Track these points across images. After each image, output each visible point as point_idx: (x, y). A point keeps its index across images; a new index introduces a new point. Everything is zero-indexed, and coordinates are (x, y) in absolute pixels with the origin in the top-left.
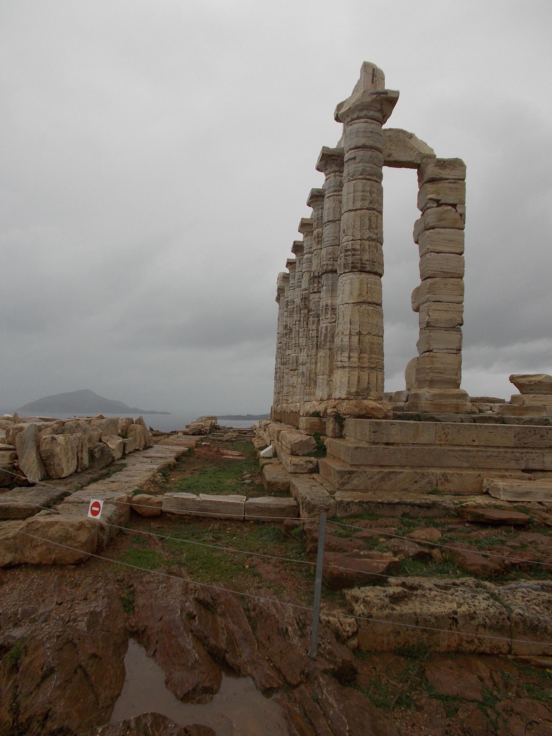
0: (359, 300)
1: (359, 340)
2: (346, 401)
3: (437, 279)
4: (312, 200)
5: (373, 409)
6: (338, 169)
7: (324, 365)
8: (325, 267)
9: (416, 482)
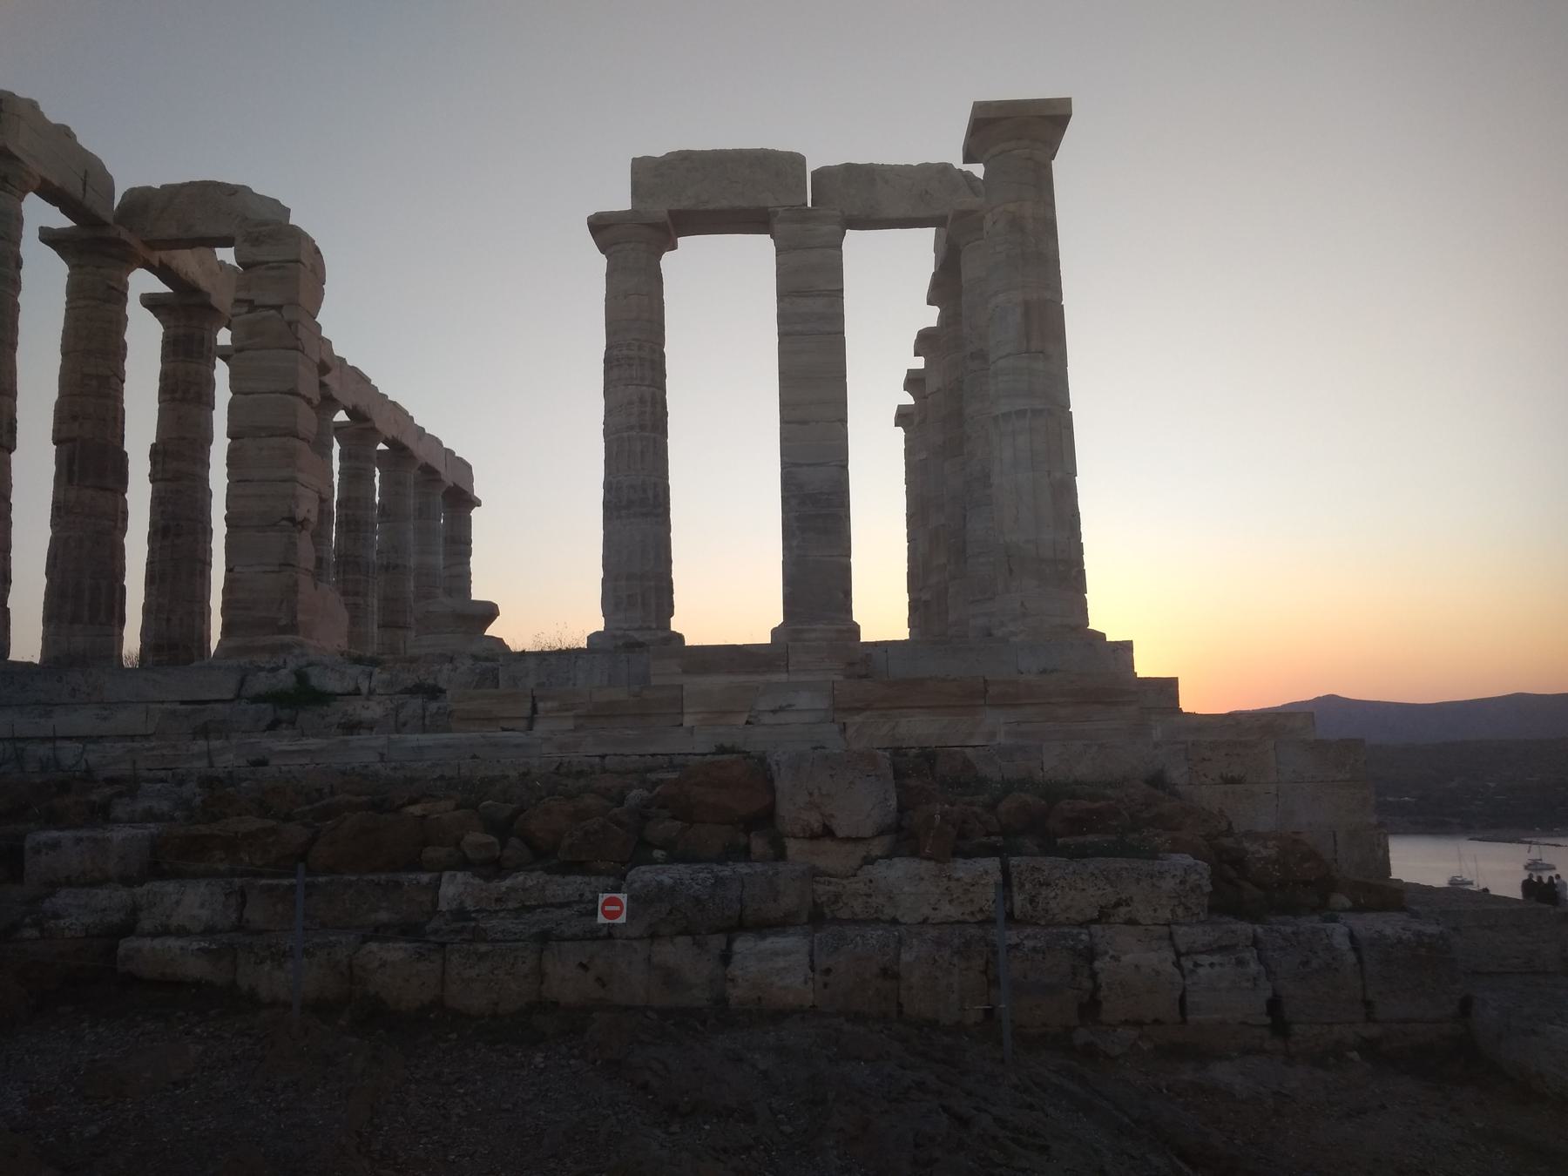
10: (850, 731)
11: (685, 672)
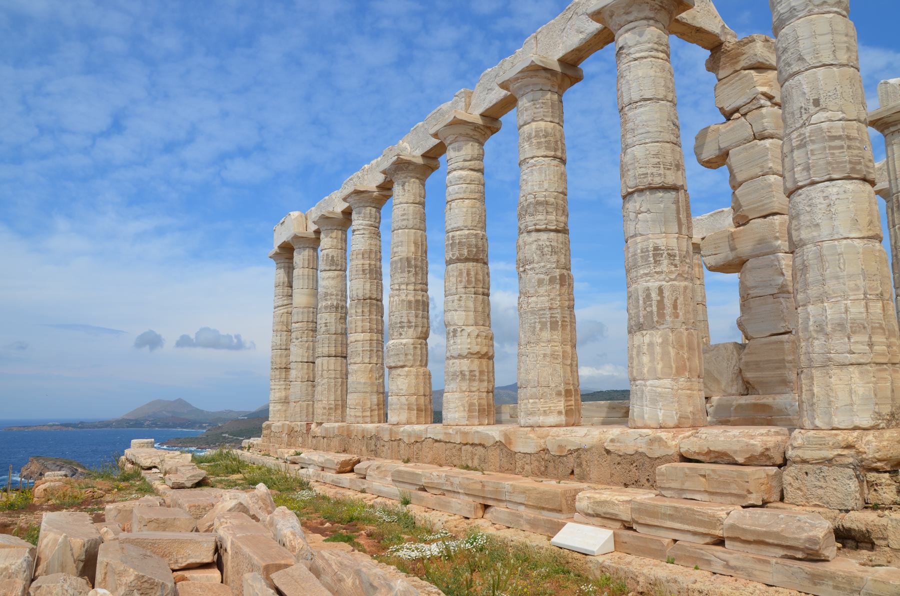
0: (871, 233)
1: (884, 310)
2: (872, 432)
4: (526, 74)
6: (652, 16)
7: (662, 359)
8: (650, 179)
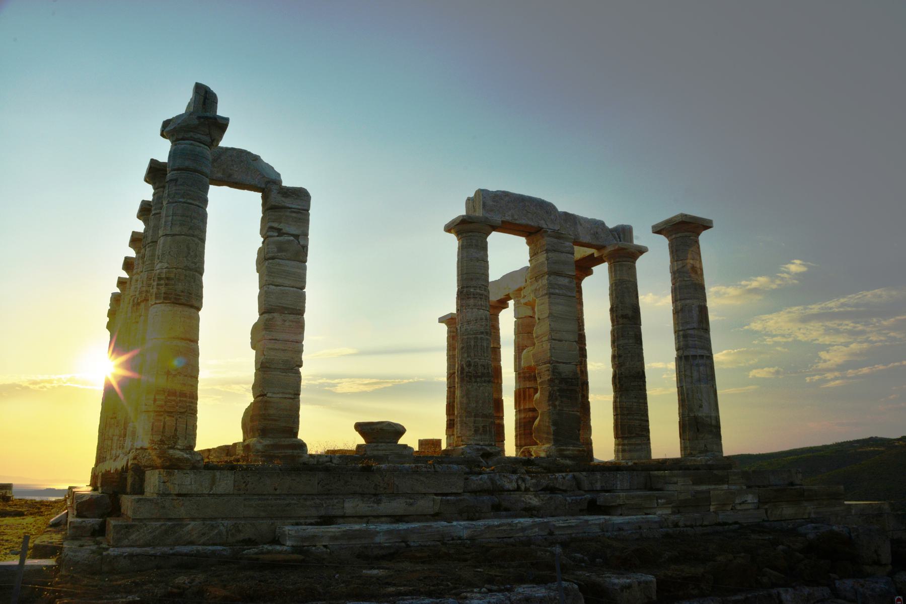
3: (275, 315)
5: (178, 459)
9: (204, 534)
10: (769, 512)
11: (694, 484)
